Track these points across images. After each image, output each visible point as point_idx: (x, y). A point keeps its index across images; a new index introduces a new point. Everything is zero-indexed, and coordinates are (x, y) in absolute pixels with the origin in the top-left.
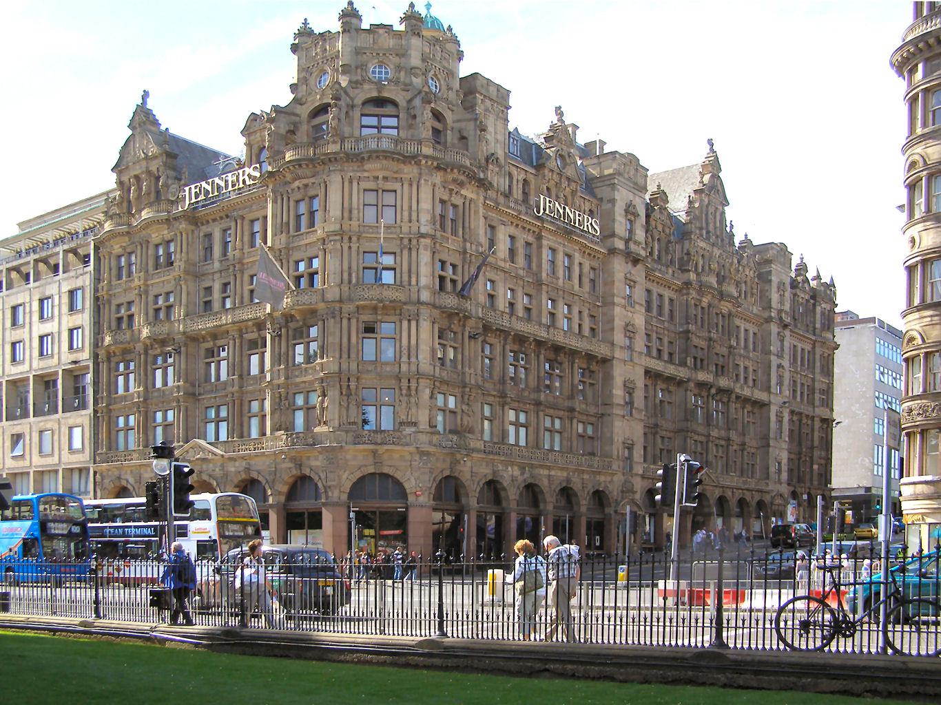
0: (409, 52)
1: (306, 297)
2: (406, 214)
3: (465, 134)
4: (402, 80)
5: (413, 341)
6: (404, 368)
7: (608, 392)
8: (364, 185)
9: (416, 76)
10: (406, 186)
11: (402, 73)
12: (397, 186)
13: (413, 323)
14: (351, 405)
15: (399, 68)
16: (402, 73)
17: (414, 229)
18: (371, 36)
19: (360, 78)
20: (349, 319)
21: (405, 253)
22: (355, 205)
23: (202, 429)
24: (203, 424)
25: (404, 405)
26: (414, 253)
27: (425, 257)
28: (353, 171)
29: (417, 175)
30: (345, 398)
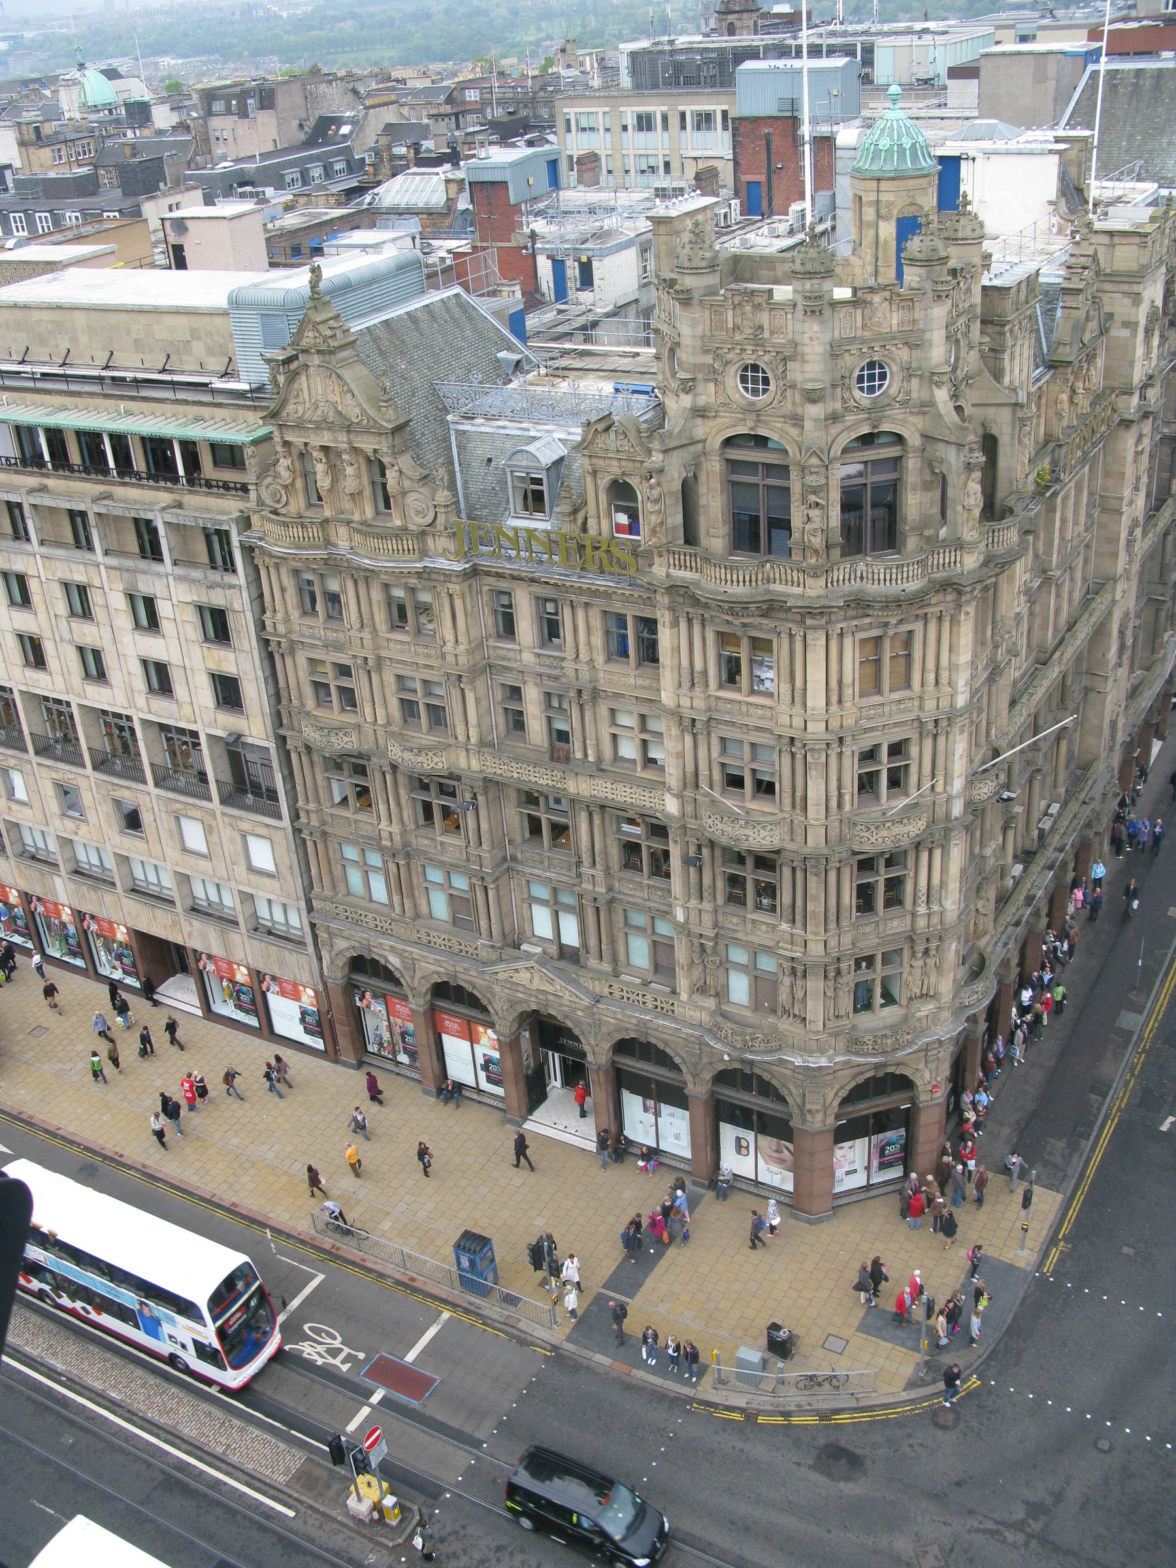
0: (928, 336)
1: (763, 833)
2: (931, 677)
3: (994, 431)
4: (914, 395)
5: (936, 880)
6: (921, 923)
7: (1100, 655)
8: (861, 635)
9: (938, 385)
10: (932, 627)
11: (915, 382)
12: (918, 627)
13: (937, 853)
14: (841, 993)
15: (909, 372)
16: (915, 382)
17: (945, 703)
18: (859, 311)
19: (838, 406)
20: (839, 869)
21: (928, 743)
22: (848, 679)
23: (526, 913)
24: (525, 906)
25: (918, 972)
26: (941, 740)
27: (960, 746)
28: (845, 619)
29: (952, 605)
30: (831, 984)
